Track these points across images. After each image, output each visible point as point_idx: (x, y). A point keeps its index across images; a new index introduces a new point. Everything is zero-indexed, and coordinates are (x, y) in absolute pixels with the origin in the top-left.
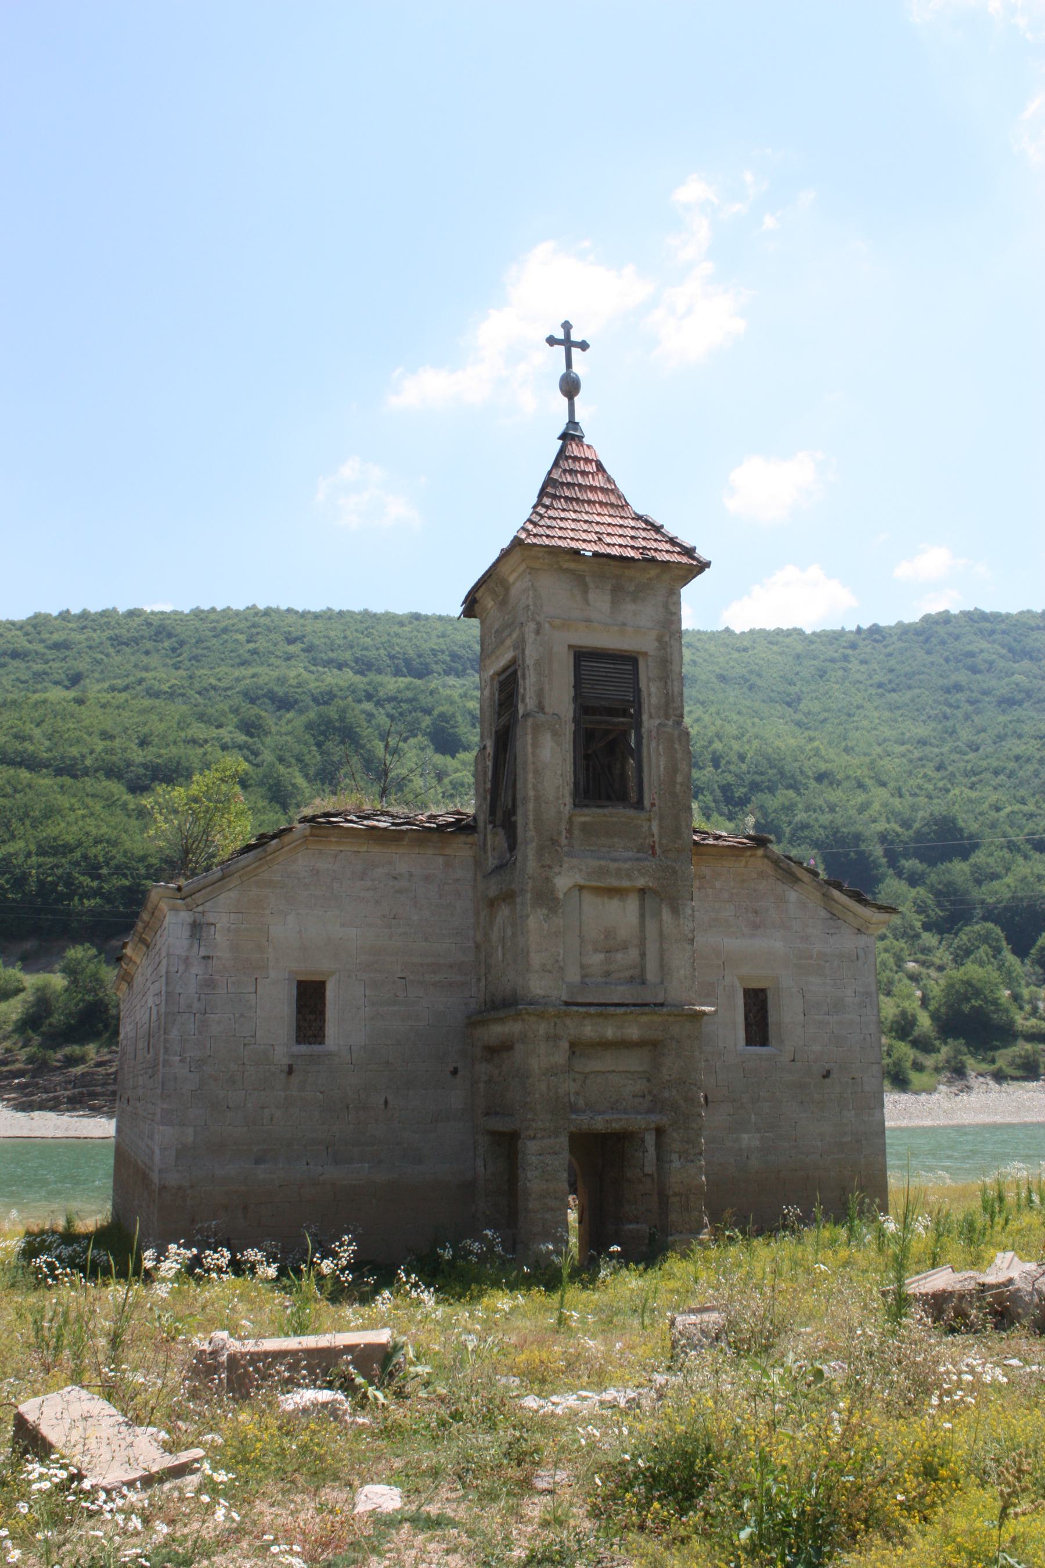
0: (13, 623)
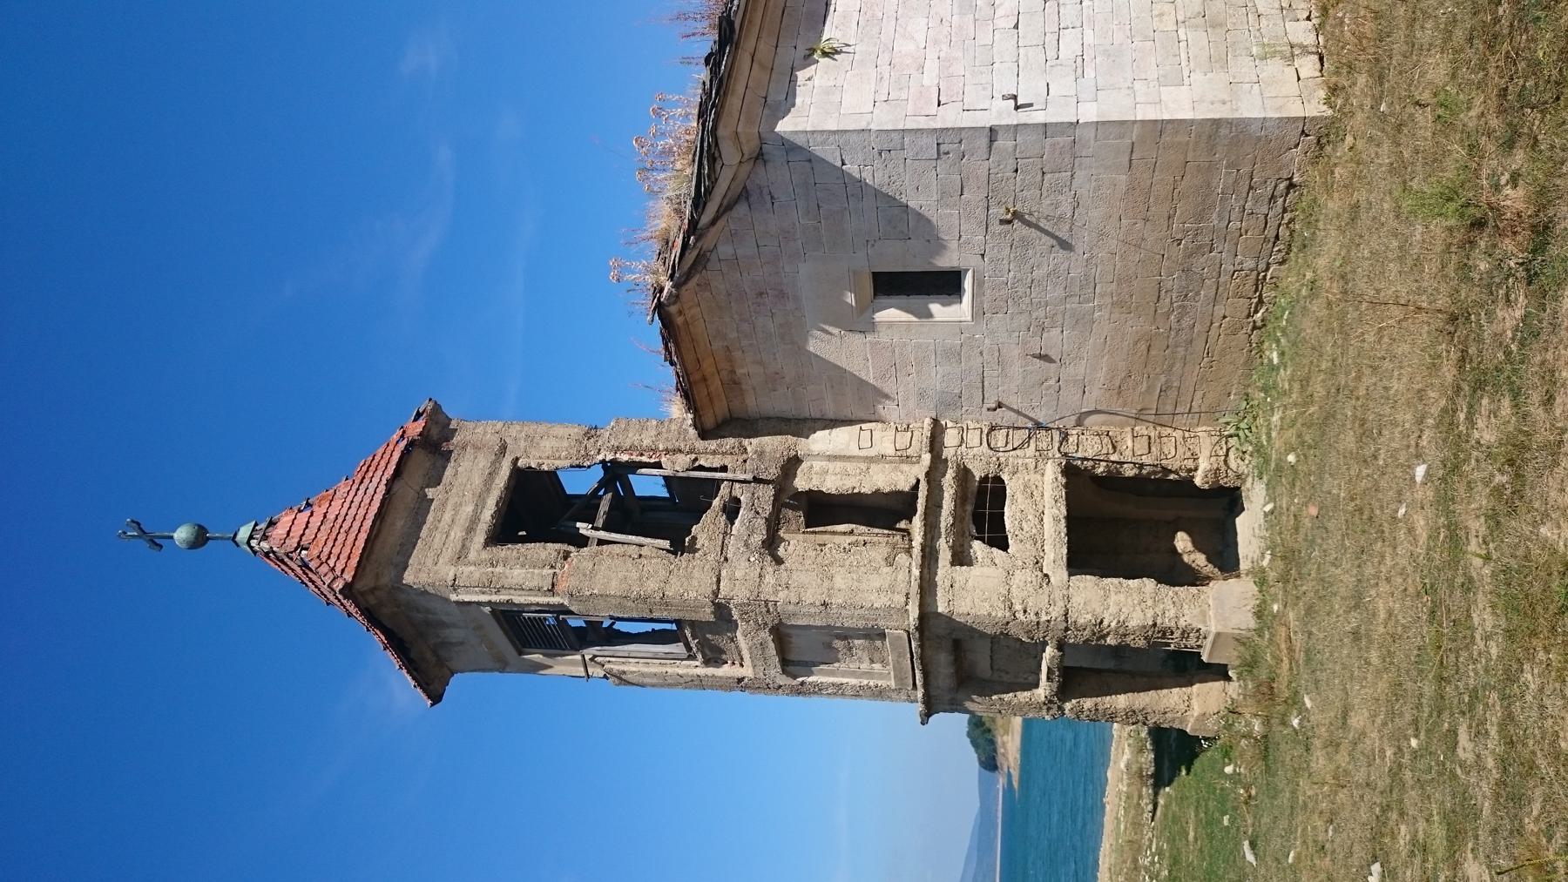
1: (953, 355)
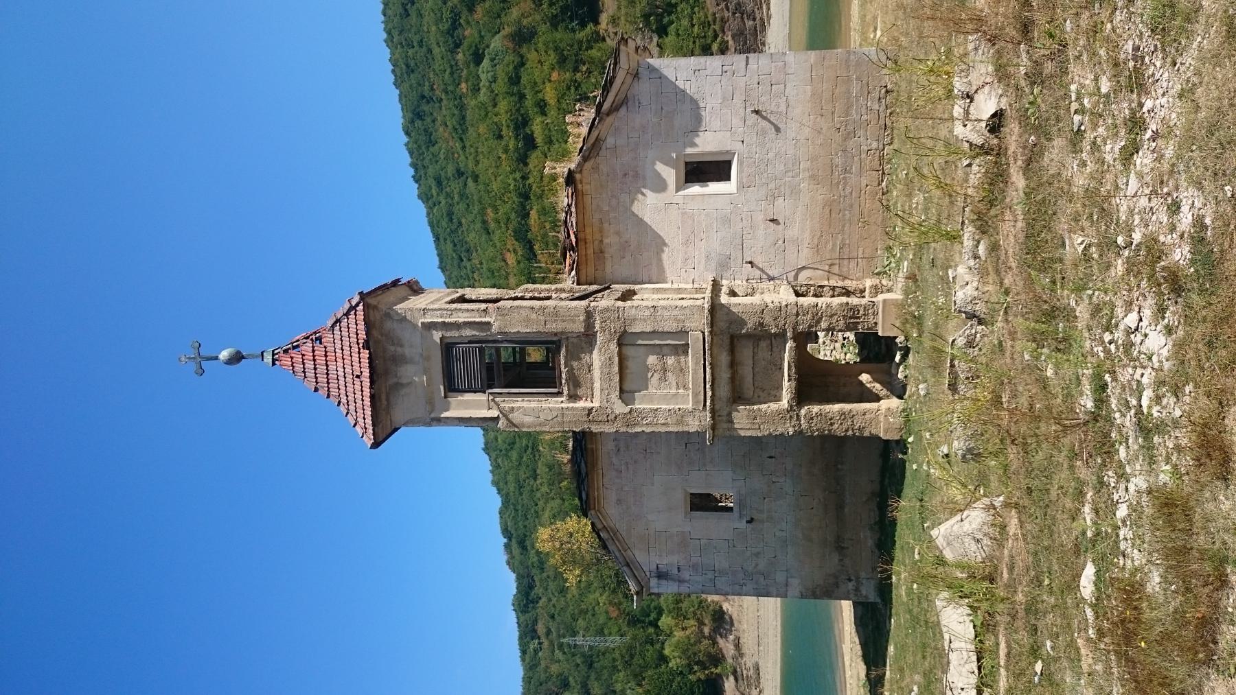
0: (428, 214)
1: (726, 221)
